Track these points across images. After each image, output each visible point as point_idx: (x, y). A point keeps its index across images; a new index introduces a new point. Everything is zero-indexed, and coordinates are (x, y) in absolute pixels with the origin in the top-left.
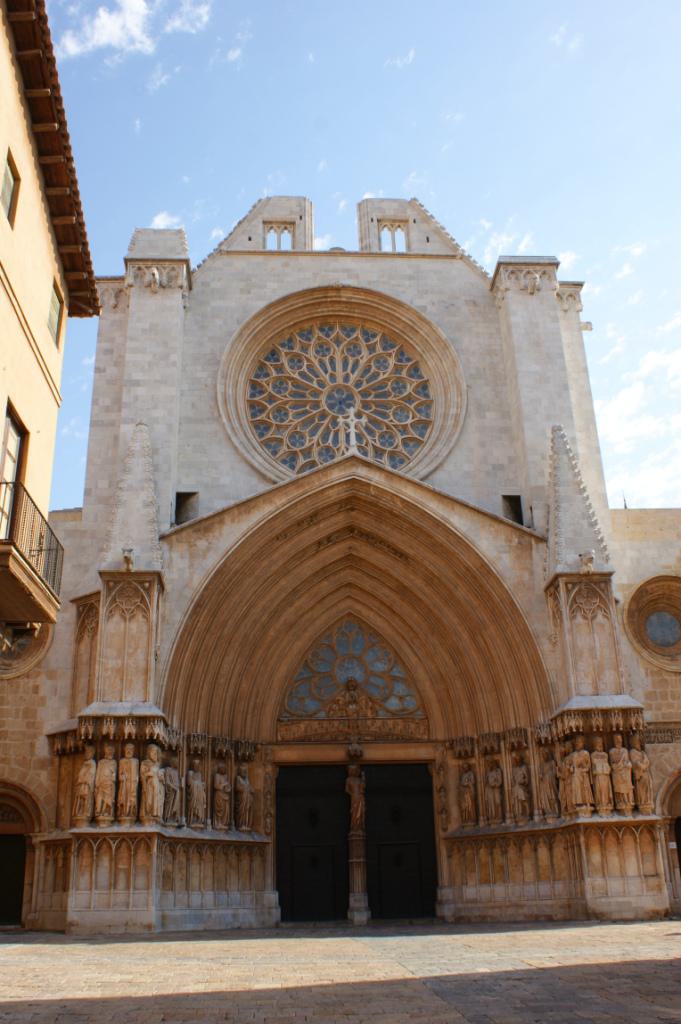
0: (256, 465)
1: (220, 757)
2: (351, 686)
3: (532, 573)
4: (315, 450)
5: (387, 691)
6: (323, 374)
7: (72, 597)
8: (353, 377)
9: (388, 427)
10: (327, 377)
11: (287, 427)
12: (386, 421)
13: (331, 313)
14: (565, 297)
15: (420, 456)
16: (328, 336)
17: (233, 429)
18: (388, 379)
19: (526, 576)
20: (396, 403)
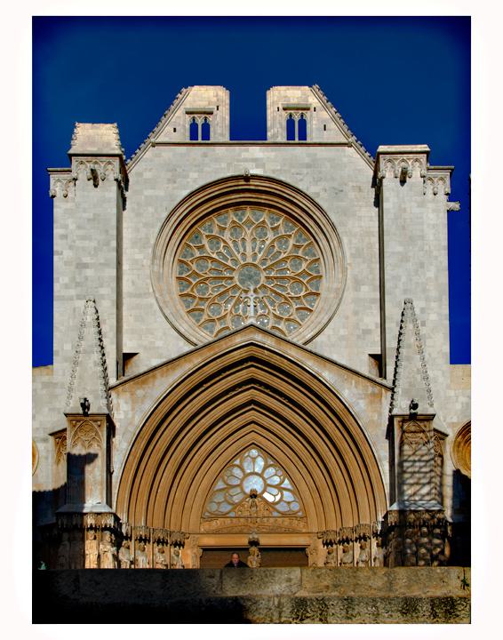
0: (182, 331)
1: (159, 542)
2: (254, 495)
3: (380, 414)
4: (229, 318)
5: (278, 498)
6: (236, 253)
7: (51, 432)
8: (260, 256)
9: (286, 298)
10: (239, 256)
11: (207, 299)
12: (283, 293)
13: (242, 200)
14: (435, 180)
15: (308, 324)
16: (241, 220)
17: (165, 302)
18: (287, 258)
19: (376, 417)
20: (293, 278)
